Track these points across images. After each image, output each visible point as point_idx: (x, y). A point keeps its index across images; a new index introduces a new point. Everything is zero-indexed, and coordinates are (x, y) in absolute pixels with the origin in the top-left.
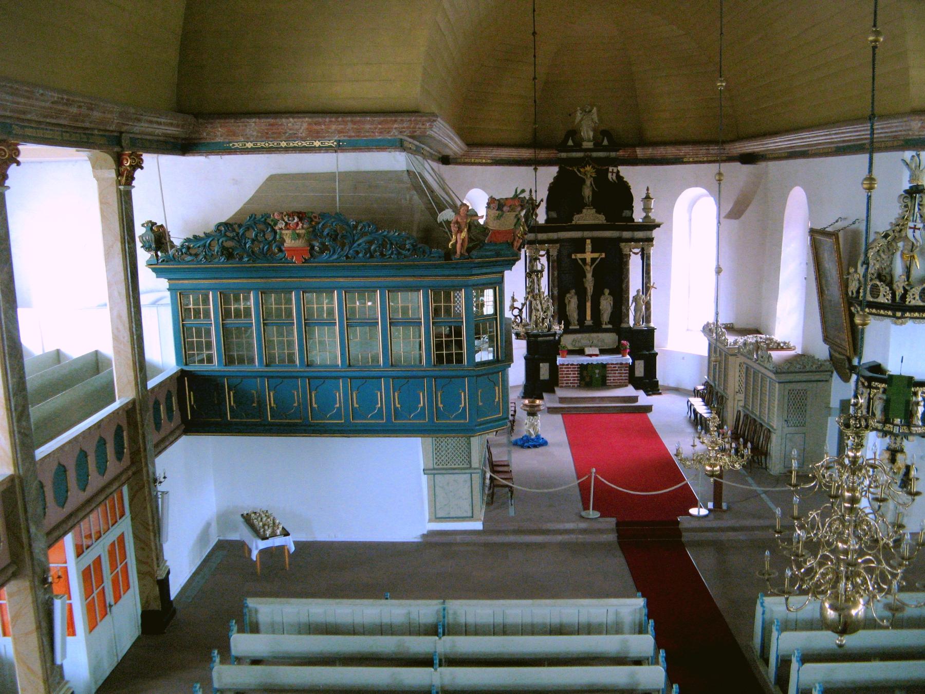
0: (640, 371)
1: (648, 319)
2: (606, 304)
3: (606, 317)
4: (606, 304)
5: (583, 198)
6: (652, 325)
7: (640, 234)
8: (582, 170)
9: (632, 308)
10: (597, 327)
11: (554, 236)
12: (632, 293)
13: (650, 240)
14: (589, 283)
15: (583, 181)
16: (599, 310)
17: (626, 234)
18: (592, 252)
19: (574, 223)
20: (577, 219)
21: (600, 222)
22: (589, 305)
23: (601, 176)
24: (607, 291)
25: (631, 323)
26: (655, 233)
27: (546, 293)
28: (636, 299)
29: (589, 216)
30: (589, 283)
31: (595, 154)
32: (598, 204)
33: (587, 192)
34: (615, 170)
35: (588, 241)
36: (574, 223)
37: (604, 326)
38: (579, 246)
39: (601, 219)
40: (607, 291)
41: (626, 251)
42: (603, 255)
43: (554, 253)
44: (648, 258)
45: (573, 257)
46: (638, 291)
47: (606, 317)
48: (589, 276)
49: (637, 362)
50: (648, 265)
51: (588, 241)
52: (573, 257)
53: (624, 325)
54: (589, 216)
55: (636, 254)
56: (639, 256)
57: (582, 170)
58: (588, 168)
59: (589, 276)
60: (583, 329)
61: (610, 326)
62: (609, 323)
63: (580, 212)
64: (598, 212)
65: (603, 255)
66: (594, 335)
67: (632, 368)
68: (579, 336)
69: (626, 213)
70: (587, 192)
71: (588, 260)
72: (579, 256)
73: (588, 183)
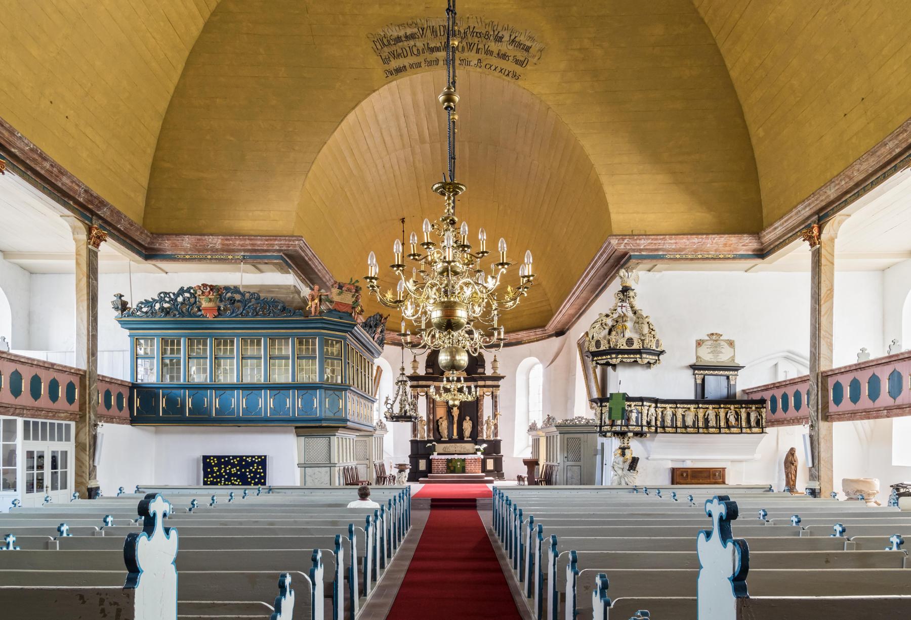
1: (496, 435)
2: (467, 426)
3: (467, 433)
4: (467, 426)
6: (499, 438)
9: (485, 427)
10: (461, 439)
12: (485, 418)
22: (455, 426)
24: (468, 418)
27: (425, 418)
28: (487, 423)
40: (468, 418)
47: (467, 433)
60: (451, 441)
66: (458, 445)
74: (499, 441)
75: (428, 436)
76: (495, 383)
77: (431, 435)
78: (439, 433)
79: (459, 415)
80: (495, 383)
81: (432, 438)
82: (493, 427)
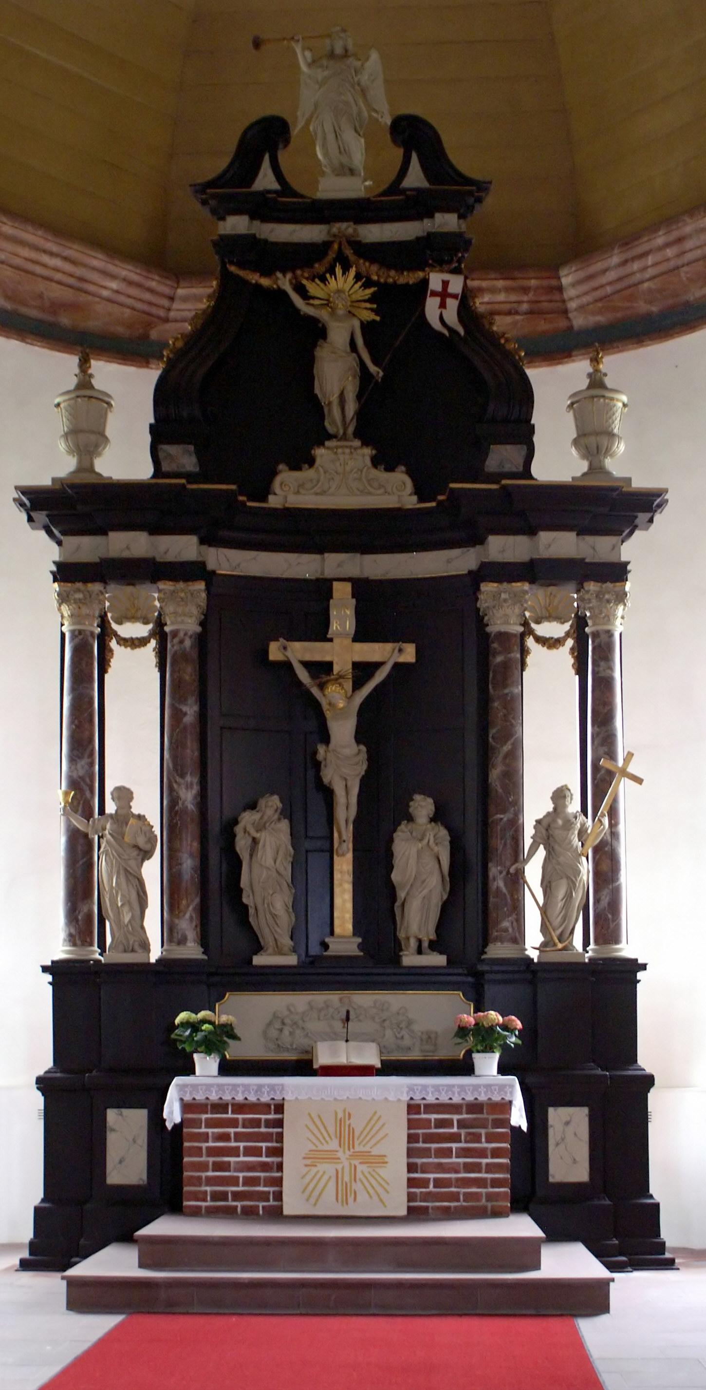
0: (570, 1148)
2: (420, 858)
4: (420, 858)
5: (317, 409)
7: (559, 544)
8: (313, 288)
11: (183, 547)
13: (618, 572)
14: (344, 762)
15: (316, 331)
16: (391, 891)
17: (504, 548)
18: (361, 635)
19: (274, 502)
20: (291, 490)
21: (389, 501)
23: (397, 307)
24: (423, 807)
25: (533, 939)
26: (633, 549)
27: (148, 805)
28: (550, 830)
29: (342, 477)
30: (344, 762)
31: (375, 233)
32: (384, 432)
33: (336, 375)
34: (456, 284)
35: (342, 591)
36: (274, 502)
37: (410, 959)
38: (305, 611)
39: (396, 491)
40: (423, 807)
41: (503, 619)
42: (409, 654)
43: (186, 622)
44: (605, 652)
45: (275, 652)
46: (560, 796)
48: (343, 730)
49: (556, 1116)
50: (605, 685)
51: (342, 591)
52: (275, 652)
53: (497, 951)
54: (342, 477)
55: (551, 643)
56: (564, 656)
57: (313, 288)
58: (343, 284)
59: (343, 730)
60: (316, 972)
61: (439, 960)
62: (435, 946)
63: (302, 459)
64: (384, 460)
65: (409, 654)
67: (530, 1147)
68: (300, 1001)
69: (502, 457)
70: (336, 375)
71: (342, 665)
72: (299, 652)
73: (339, 333)
74: (634, 967)
75: (170, 932)
76: (597, 548)
77: (188, 925)
78: (242, 912)
79: (370, 788)
80: (597, 548)
81: (192, 951)
82: (586, 868)
